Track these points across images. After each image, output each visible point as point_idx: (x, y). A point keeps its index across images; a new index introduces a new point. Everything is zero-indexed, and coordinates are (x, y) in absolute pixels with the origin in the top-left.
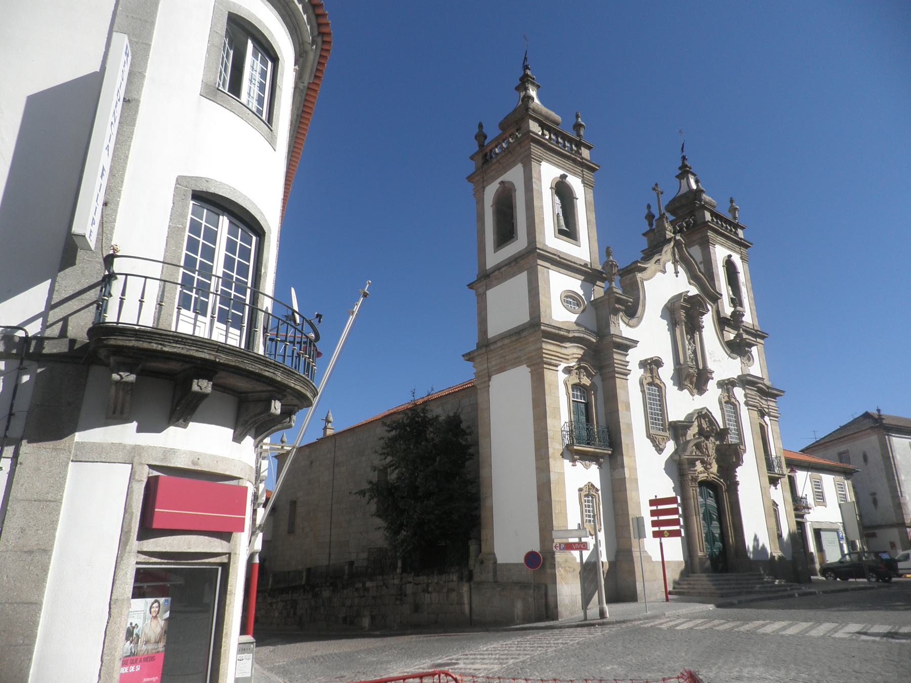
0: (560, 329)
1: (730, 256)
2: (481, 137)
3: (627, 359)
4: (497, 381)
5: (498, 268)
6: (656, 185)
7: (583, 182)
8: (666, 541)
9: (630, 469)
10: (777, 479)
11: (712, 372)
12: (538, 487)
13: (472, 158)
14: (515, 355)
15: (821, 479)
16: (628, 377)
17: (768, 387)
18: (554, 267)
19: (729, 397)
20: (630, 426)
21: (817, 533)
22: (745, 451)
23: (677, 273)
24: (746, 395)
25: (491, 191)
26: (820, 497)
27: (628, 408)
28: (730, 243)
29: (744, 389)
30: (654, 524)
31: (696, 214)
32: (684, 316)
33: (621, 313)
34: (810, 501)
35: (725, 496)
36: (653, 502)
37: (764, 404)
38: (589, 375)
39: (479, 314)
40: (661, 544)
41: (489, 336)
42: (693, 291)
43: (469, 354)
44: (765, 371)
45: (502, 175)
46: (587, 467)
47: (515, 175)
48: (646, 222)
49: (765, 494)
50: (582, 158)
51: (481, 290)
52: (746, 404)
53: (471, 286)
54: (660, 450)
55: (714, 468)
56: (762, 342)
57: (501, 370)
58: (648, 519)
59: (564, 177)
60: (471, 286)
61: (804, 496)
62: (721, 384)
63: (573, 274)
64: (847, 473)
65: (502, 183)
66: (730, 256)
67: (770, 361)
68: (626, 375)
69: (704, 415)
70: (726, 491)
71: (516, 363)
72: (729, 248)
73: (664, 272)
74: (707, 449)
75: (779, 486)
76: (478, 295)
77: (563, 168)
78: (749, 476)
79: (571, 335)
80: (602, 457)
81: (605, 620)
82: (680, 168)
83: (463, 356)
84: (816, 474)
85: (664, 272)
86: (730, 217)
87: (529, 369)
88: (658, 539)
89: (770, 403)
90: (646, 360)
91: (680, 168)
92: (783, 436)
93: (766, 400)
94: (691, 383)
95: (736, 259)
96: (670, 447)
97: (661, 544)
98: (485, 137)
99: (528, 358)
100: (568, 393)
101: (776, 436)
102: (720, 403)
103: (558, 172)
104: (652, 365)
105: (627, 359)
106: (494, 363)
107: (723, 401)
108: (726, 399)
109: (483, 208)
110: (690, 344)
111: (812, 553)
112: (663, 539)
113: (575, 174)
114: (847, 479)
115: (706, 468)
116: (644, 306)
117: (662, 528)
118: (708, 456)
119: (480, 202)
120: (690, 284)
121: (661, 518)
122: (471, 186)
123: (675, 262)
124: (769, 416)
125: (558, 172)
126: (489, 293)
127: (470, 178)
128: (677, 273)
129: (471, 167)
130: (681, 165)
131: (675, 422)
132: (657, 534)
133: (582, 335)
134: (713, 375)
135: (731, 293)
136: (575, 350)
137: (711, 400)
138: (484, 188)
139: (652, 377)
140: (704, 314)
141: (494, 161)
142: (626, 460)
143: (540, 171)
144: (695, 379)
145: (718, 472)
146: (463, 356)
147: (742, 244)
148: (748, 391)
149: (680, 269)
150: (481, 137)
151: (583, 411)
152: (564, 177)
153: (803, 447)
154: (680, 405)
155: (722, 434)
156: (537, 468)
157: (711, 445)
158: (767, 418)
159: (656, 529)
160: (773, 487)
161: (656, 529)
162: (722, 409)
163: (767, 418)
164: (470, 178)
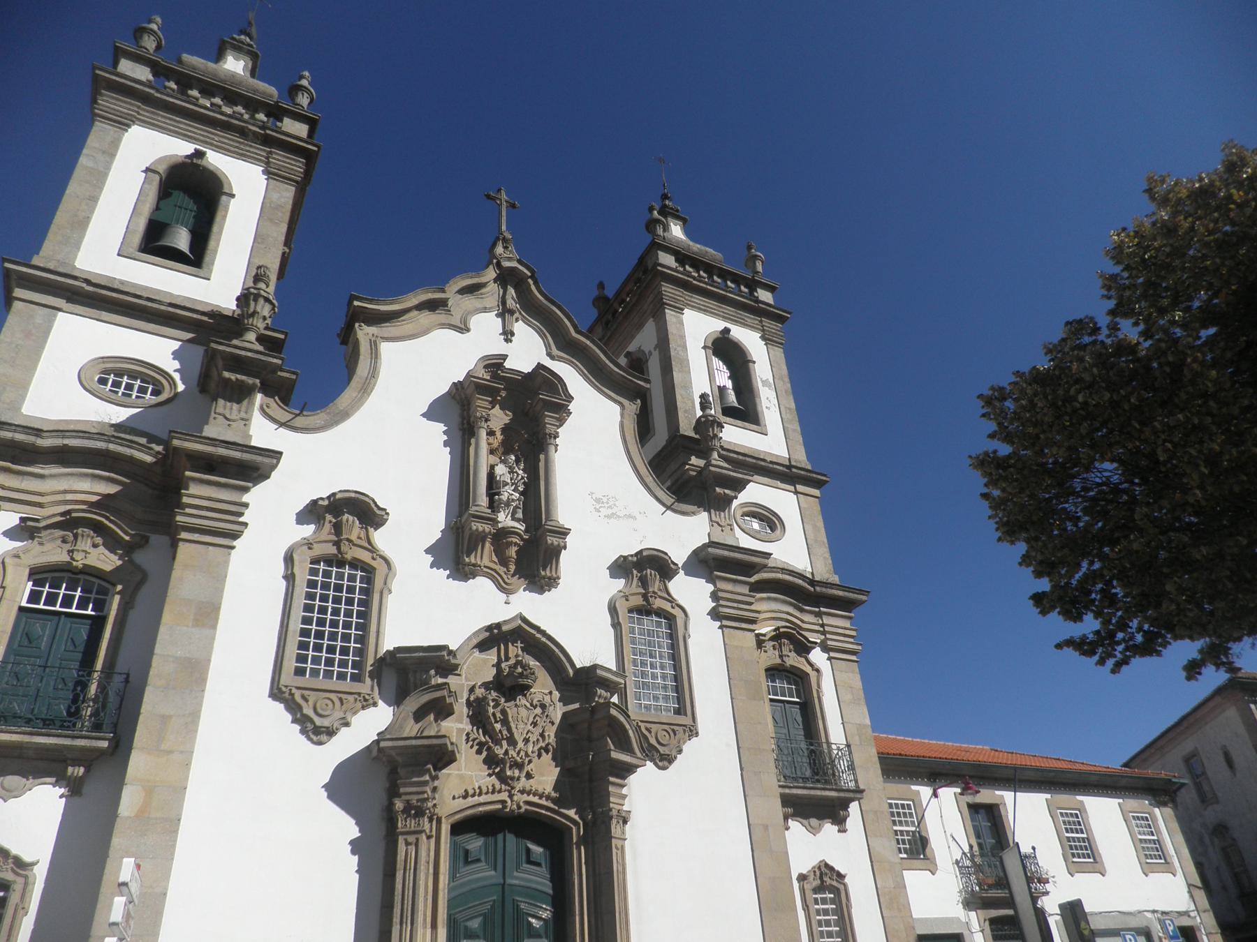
1: (727, 331)
3: (245, 498)
7: (266, 172)
9: (149, 791)
10: (845, 804)
11: (564, 533)
15: (1081, 808)
16: (235, 543)
17: (812, 582)
18: (70, 307)
19: (645, 597)
24: (714, 596)
26: (1081, 852)
27: (208, 614)
28: (730, 310)
29: (711, 579)
32: (506, 419)
33: (259, 398)
35: (579, 858)
37: (808, 620)
38: (112, 543)
44: (823, 552)
52: (715, 614)
55: (545, 776)
56: (817, 492)
59: (199, 154)
62: (621, 567)
63: (151, 326)
64: (1161, 792)
67: (838, 530)
68: (235, 536)
70: (583, 840)
72: (725, 319)
74: (505, 722)
80: (76, 762)
84: (1064, 799)
89: (827, 620)
90: (314, 503)
92: (877, 697)
93: (819, 615)
94: (504, 561)
101: (847, 697)
102: (613, 610)
104: (347, 514)
105: (245, 498)
107: (622, 608)
108: (638, 601)
114: (1160, 804)
115: (503, 779)
116: (366, 389)
118: (512, 741)
124: (826, 649)
133: (100, 445)
136: (85, 485)
144: (513, 551)
145: (555, 789)
147: (757, 311)
148: (722, 585)
154: (431, 609)
155: (581, 684)
157: (539, 714)
158: (817, 656)
160: (829, 828)
162: (616, 625)
163: (817, 656)
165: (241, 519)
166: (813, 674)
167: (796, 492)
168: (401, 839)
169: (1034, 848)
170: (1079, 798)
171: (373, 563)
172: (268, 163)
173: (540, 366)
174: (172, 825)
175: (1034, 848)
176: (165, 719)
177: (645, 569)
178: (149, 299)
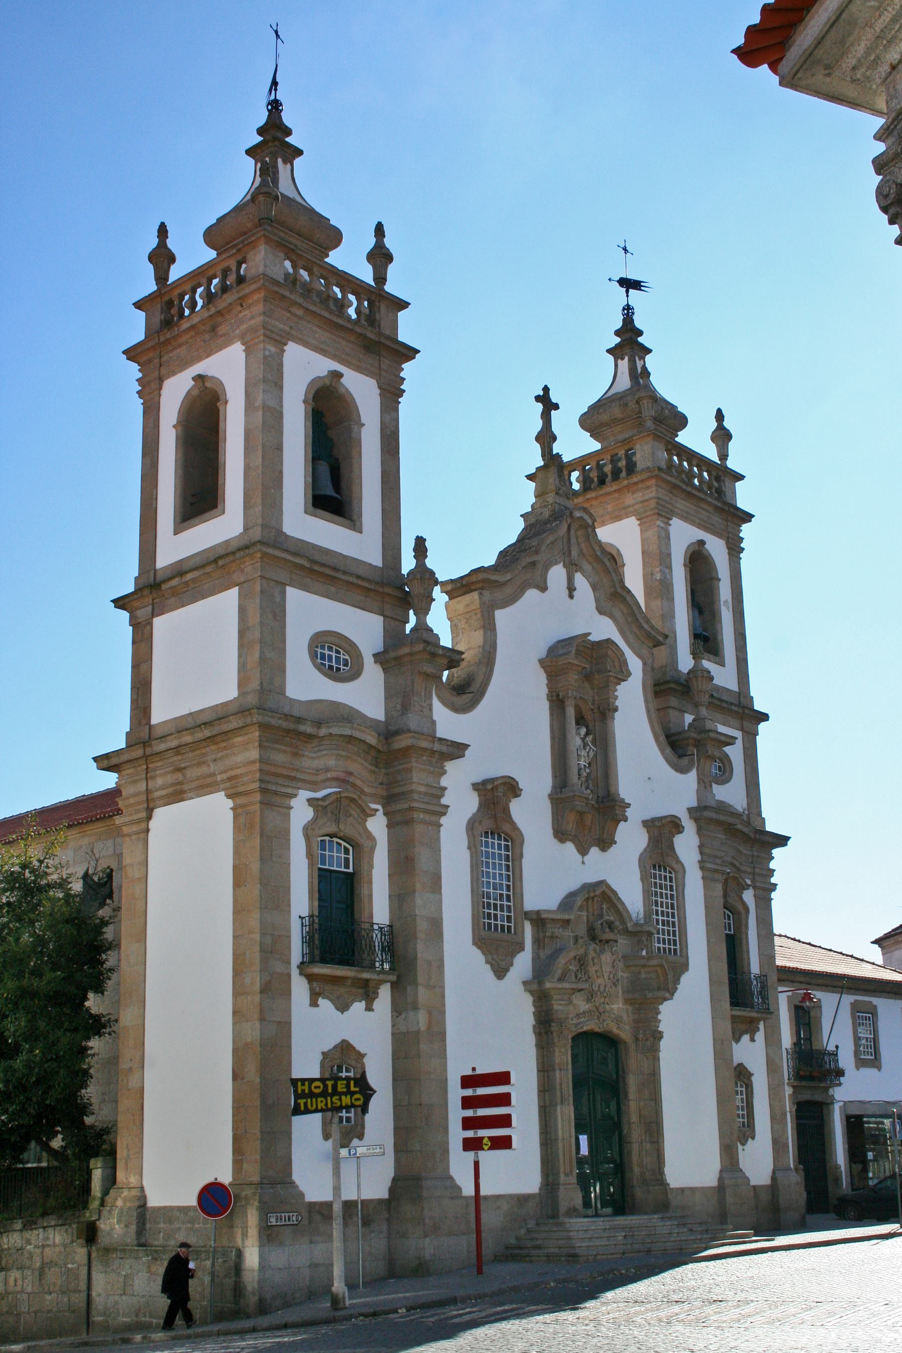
0: (299, 720)
1: (702, 543)
2: (162, 257)
3: (444, 782)
4: (165, 818)
5: (179, 570)
6: (546, 389)
8: (487, 1157)
9: (430, 1013)
12: (235, 1051)
13: (138, 305)
14: (204, 770)
16: (443, 820)
20: (436, 925)
21: (854, 1124)
22: (685, 967)
23: (571, 589)
25: (176, 390)
30: (468, 1124)
31: (638, 447)
34: (846, 1060)
36: (468, 1081)
39: (136, 666)
40: (477, 1164)
41: (155, 720)
42: (604, 629)
43: (106, 756)
45: (200, 359)
46: (343, 1008)
47: (228, 366)
48: (537, 448)
49: (722, 1054)
50: (380, 334)
51: (142, 614)
53: (120, 603)
54: (500, 972)
57: (177, 795)
58: (456, 1114)
60: (120, 603)
61: (831, 1048)
65: (200, 378)
66: (702, 543)
69: (598, 897)
71: (205, 787)
73: (543, 588)
75: (760, 1036)
76: (135, 623)
77: (334, 357)
78: (688, 1018)
79: (323, 732)
81: (338, 1314)
82: (617, 333)
83: (95, 759)
85: (543, 588)
86: (710, 452)
87: (230, 803)
88: (471, 1154)
91: (617, 333)
95: (716, 548)
96: (523, 964)
97: (477, 1164)
98: (172, 259)
99: (230, 779)
100: (310, 855)
103: (321, 365)
105: (444, 782)
106: (160, 781)
109: (157, 426)
110: (585, 745)
111: (838, 1167)
112: (480, 1153)
113: (358, 369)
117: (482, 1133)
119: (151, 412)
120: (601, 611)
121: (482, 1112)
122: (133, 370)
123: (572, 568)
124: (755, 888)
125: (321, 365)
126: (159, 622)
127: (131, 354)
128: (571, 589)
129: (136, 328)
130: (619, 325)
131: (538, 912)
132: (471, 1145)
134: (629, 812)
135: (698, 623)
137: (620, 867)
138: (161, 380)
139: (495, 817)
140: (620, 680)
141: (185, 325)
142: (423, 994)
143: (281, 365)
146: (95, 759)
149: (580, 580)
150: (162, 257)
151: (339, 892)
152: (337, 375)
153: (880, 934)
156: (235, 1013)
159: (470, 1134)
161: (470, 1134)
164: (131, 354)
165: (444, 801)
166: (743, 911)
167: (742, 729)
168: (557, 1050)
169: (837, 1047)
170: (875, 1001)
171: (513, 834)
172: (380, 375)
173: (609, 642)
174: (443, 1035)
175: (837, 1047)
176: (429, 963)
177: (662, 830)
178: (345, 573)
